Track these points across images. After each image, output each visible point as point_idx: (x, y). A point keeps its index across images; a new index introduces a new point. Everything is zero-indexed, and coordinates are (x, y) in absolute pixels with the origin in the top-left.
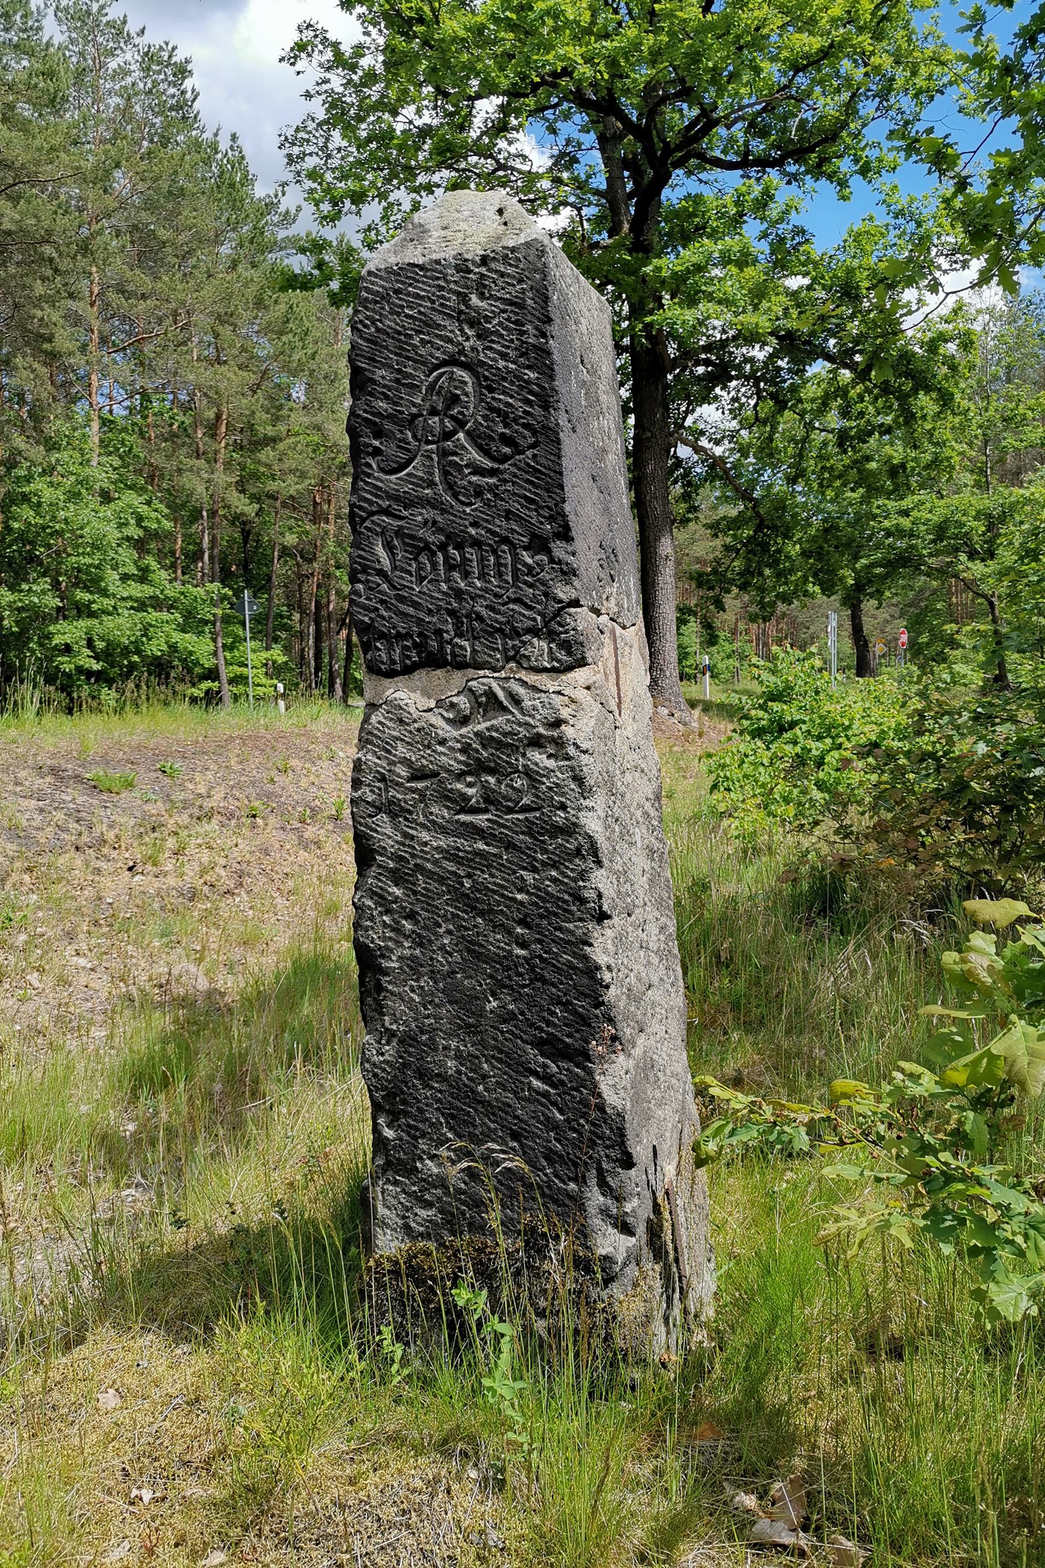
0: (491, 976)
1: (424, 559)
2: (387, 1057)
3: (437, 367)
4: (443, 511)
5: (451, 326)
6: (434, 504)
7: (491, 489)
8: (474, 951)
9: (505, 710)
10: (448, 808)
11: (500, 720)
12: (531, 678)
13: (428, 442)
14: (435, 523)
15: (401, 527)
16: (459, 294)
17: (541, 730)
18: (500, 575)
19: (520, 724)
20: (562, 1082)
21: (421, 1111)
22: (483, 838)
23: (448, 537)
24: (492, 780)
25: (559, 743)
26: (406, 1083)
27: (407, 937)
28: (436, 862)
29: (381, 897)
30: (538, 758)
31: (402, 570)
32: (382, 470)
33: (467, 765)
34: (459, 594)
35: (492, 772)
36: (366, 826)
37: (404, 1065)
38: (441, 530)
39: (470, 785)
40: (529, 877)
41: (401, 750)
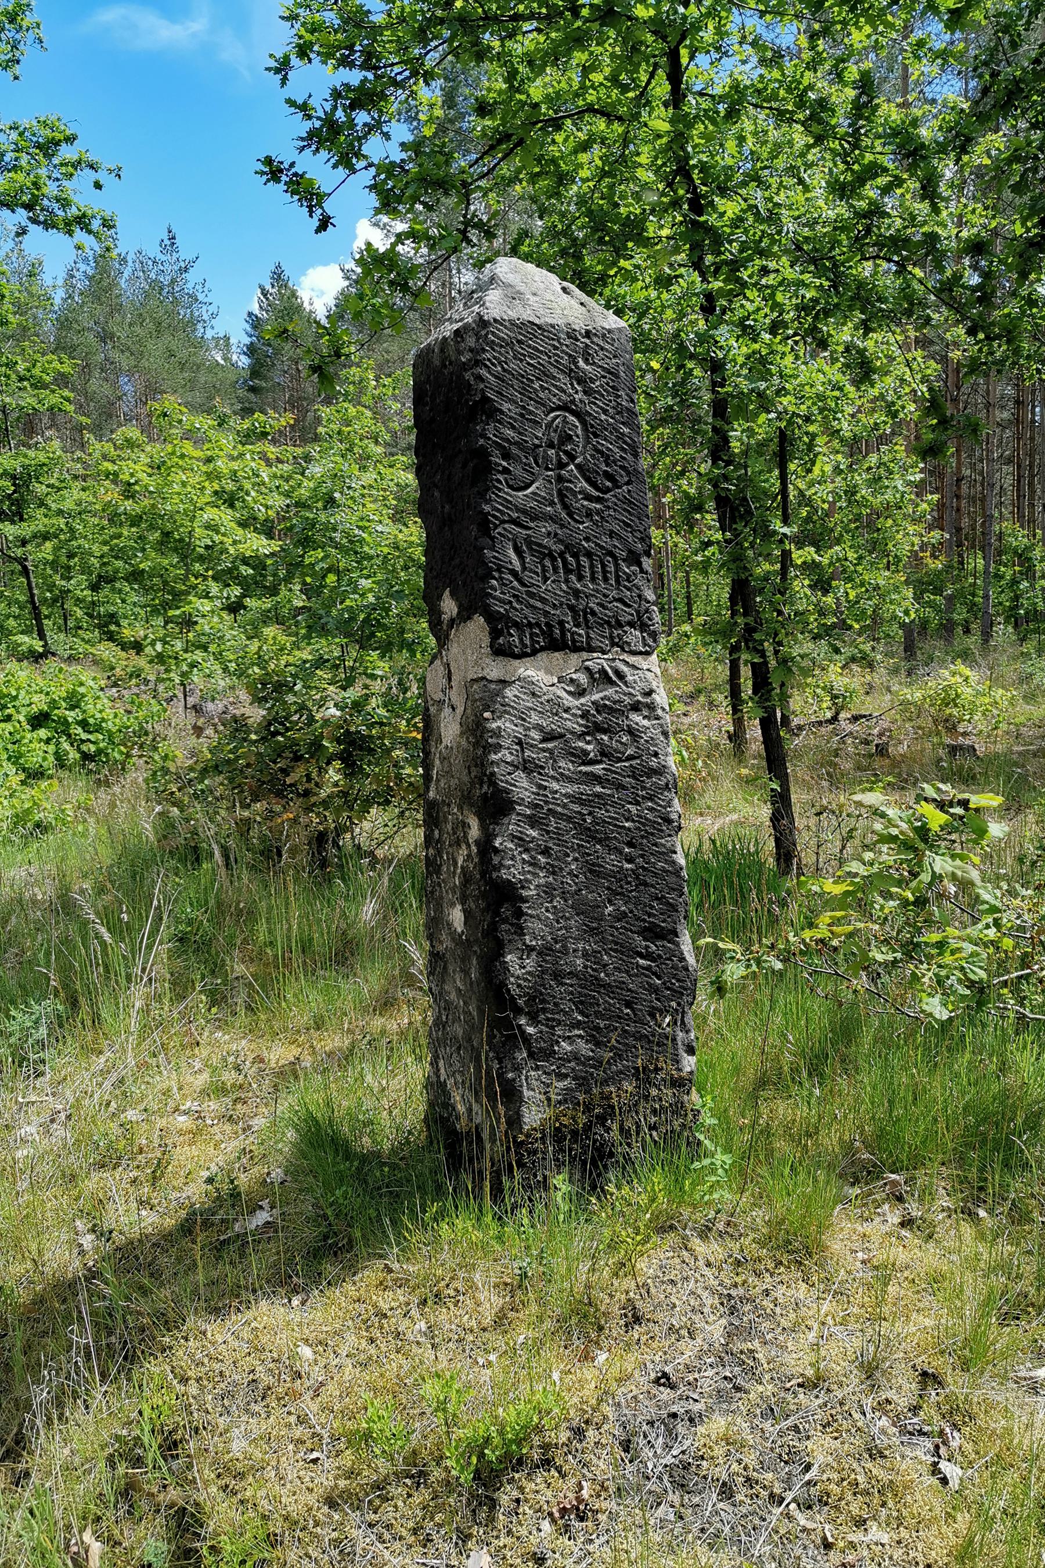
0: (608, 889)
1: (547, 563)
2: (529, 969)
3: (553, 410)
4: (562, 526)
5: (564, 380)
6: (553, 519)
7: (598, 512)
8: (594, 870)
9: (612, 683)
10: (573, 762)
11: (610, 691)
12: (631, 659)
13: (548, 469)
14: (556, 534)
15: (529, 536)
16: (570, 356)
17: (640, 698)
18: (606, 580)
19: (625, 694)
20: (659, 956)
21: (556, 1004)
22: (600, 783)
23: (566, 547)
24: (606, 738)
25: (651, 707)
26: (543, 985)
27: (541, 868)
28: (564, 806)
29: (520, 839)
30: (636, 718)
31: (531, 571)
32: (510, 487)
33: (587, 727)
34: (576, 593)
35: (605, 731)
36: (507, 782)
37: (542, 972)
38: (561, 541)
39: (588, 743)
40: (633, 809)
41: (534, 718)
